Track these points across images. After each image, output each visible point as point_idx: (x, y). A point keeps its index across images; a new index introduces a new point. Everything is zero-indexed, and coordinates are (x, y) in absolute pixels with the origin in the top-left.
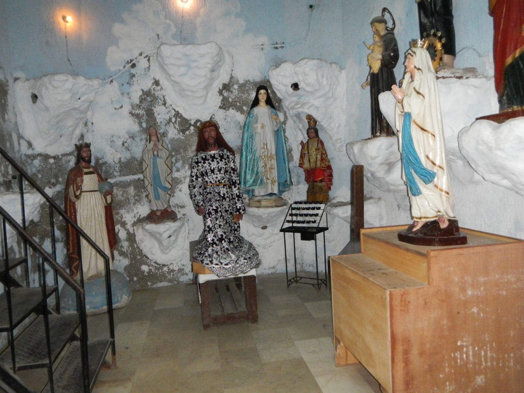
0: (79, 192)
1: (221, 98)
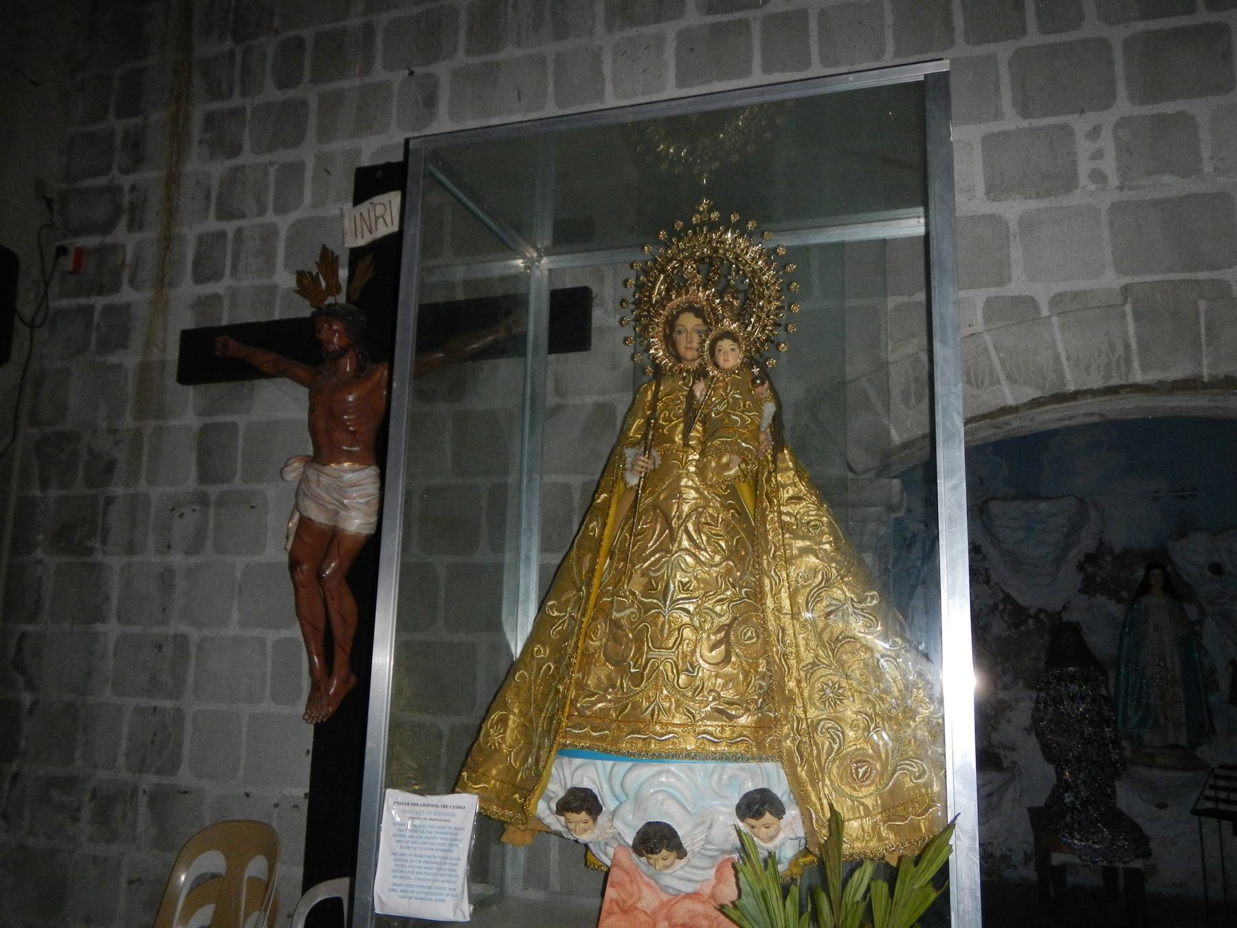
1: (1082, 575)
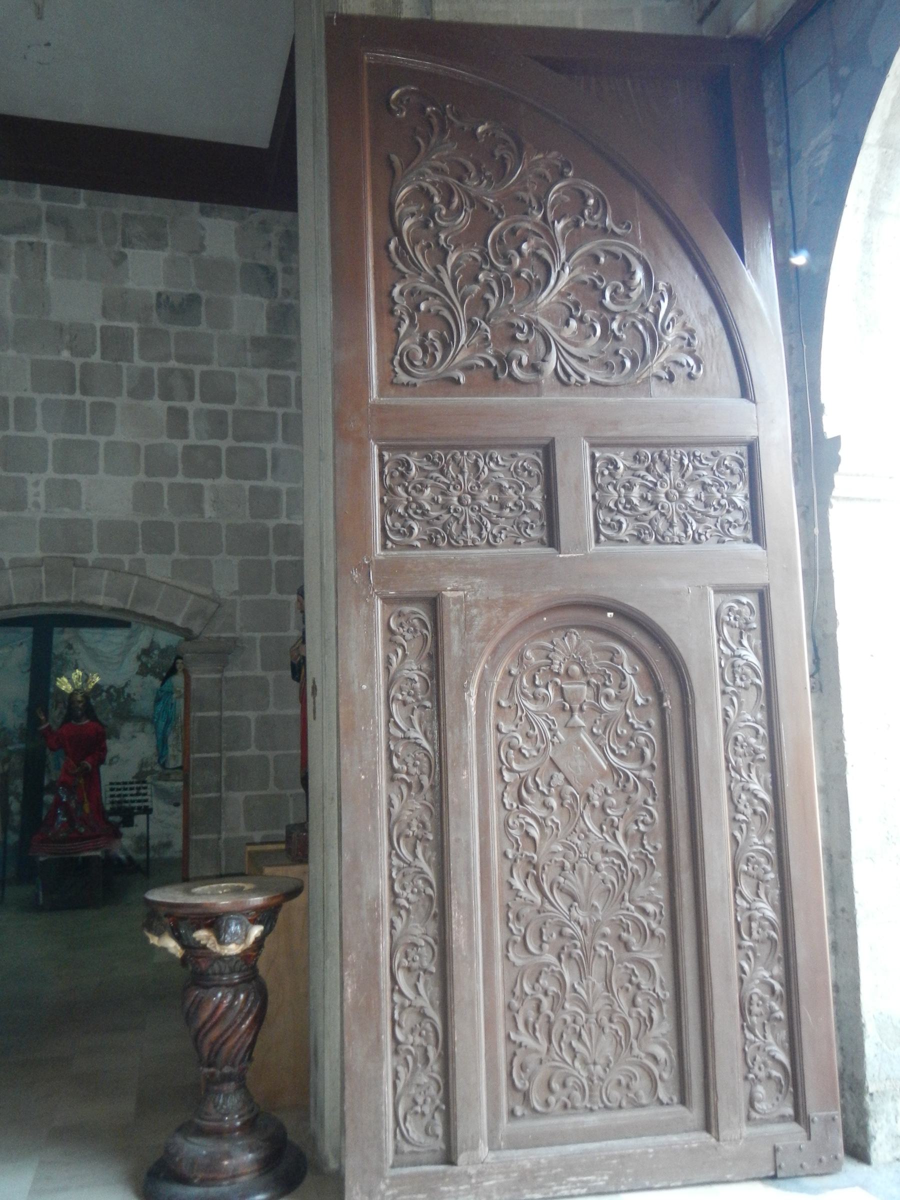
1: (139, 663)
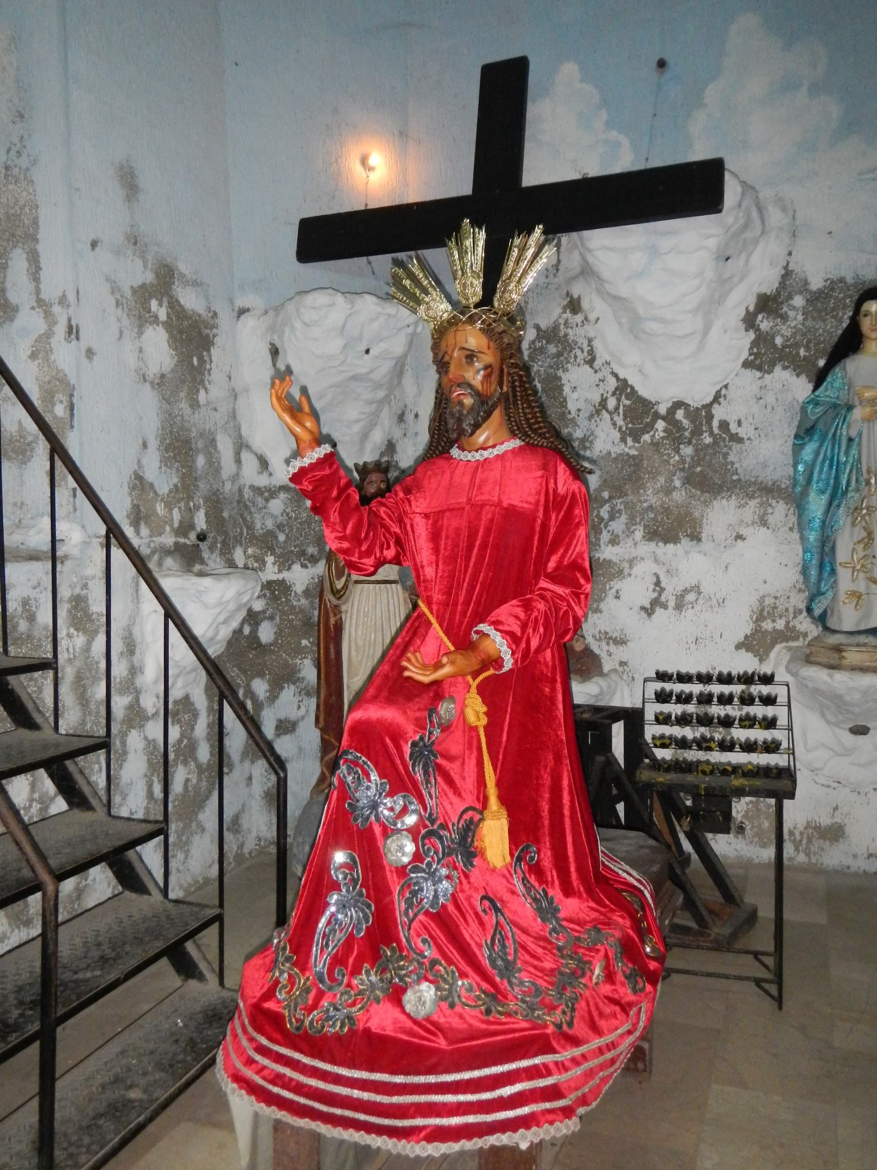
0: (344, 579)
1: (752, 335)
